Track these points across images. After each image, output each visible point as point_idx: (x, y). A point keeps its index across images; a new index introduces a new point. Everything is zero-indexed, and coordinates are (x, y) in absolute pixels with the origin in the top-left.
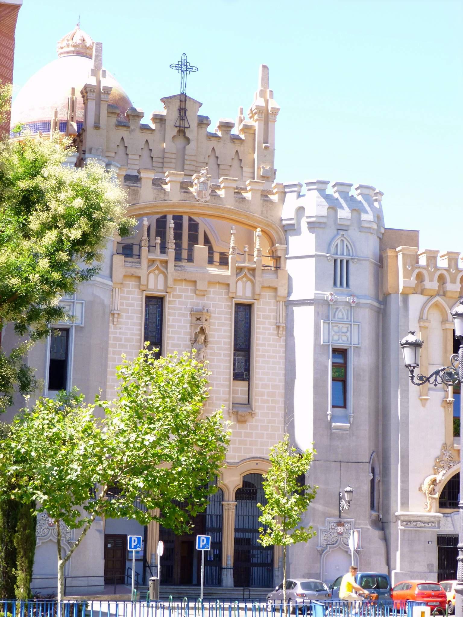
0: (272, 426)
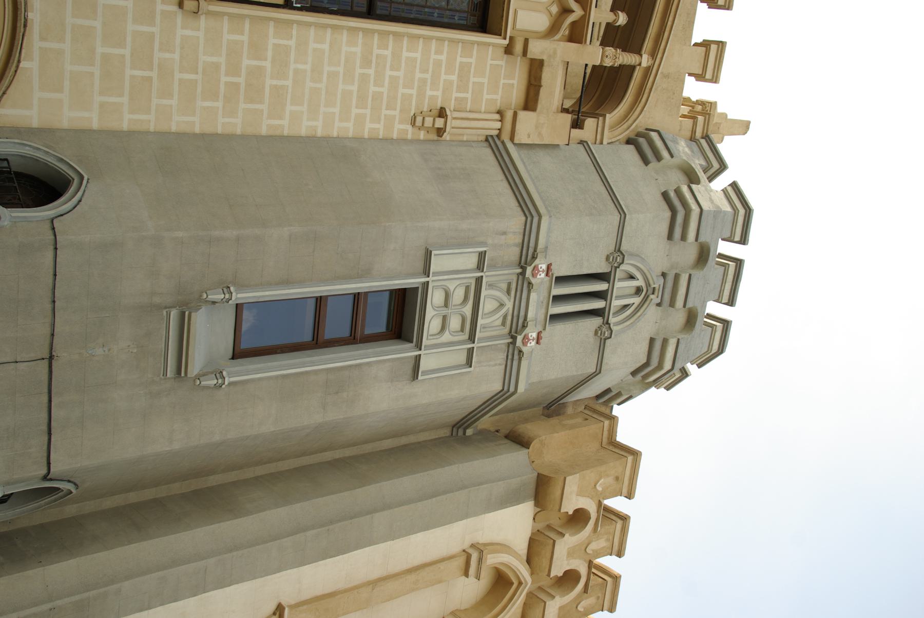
0: (150, 79)
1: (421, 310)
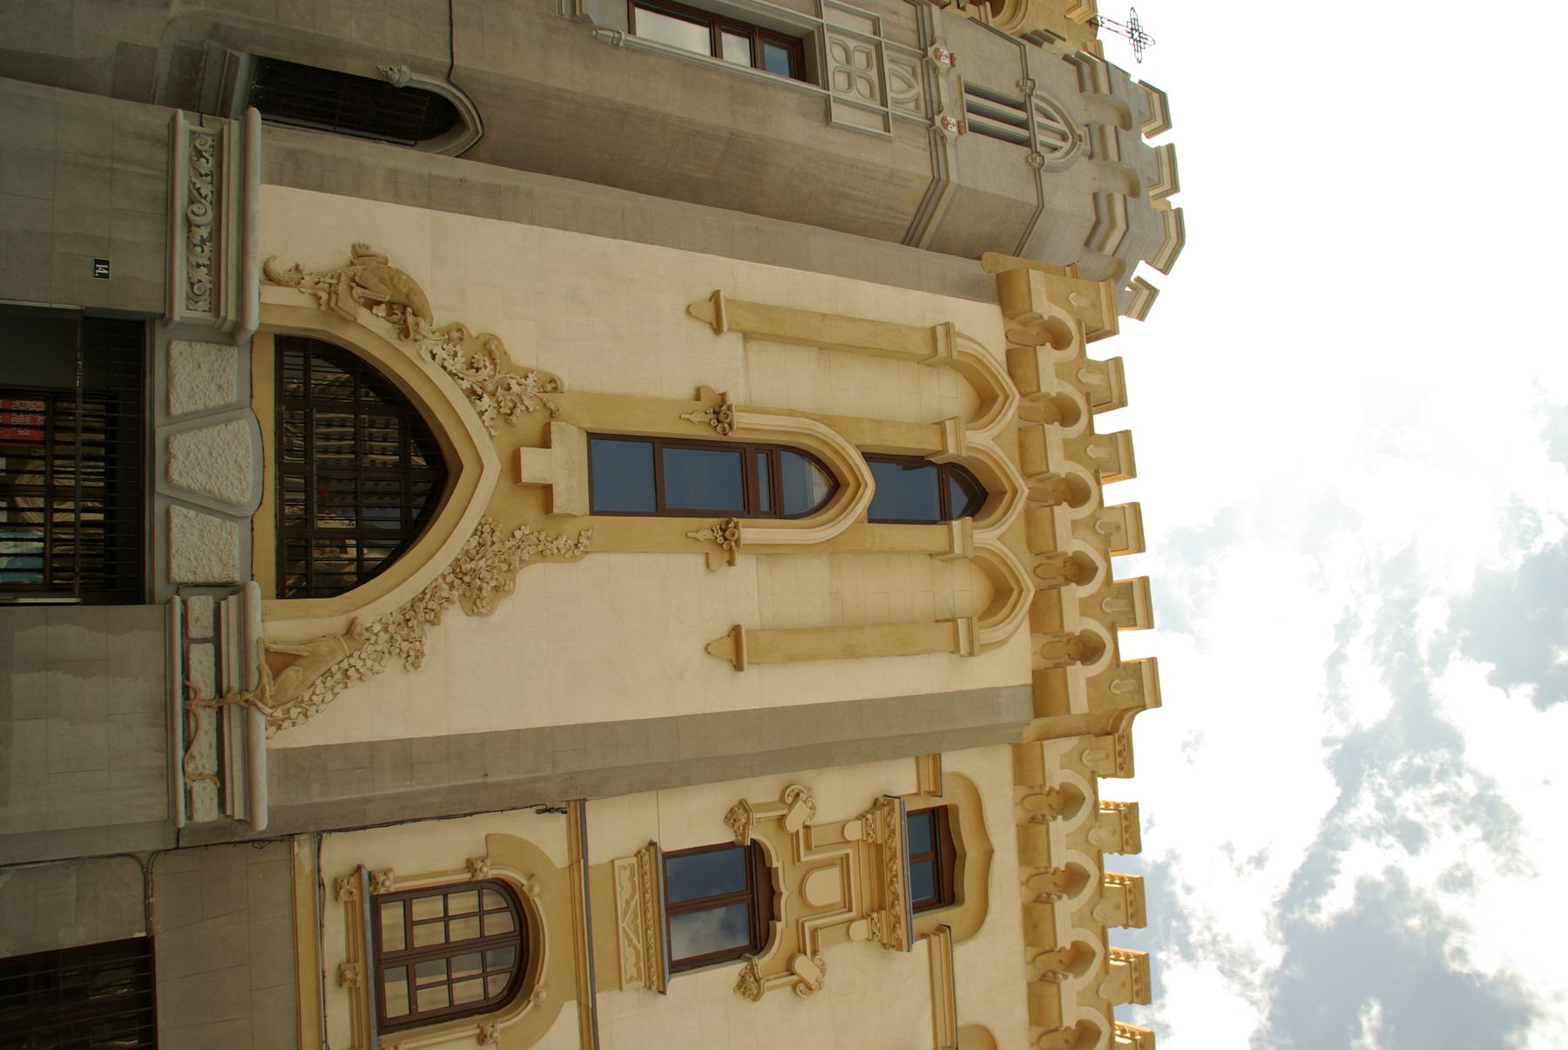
1: (822, 69)
